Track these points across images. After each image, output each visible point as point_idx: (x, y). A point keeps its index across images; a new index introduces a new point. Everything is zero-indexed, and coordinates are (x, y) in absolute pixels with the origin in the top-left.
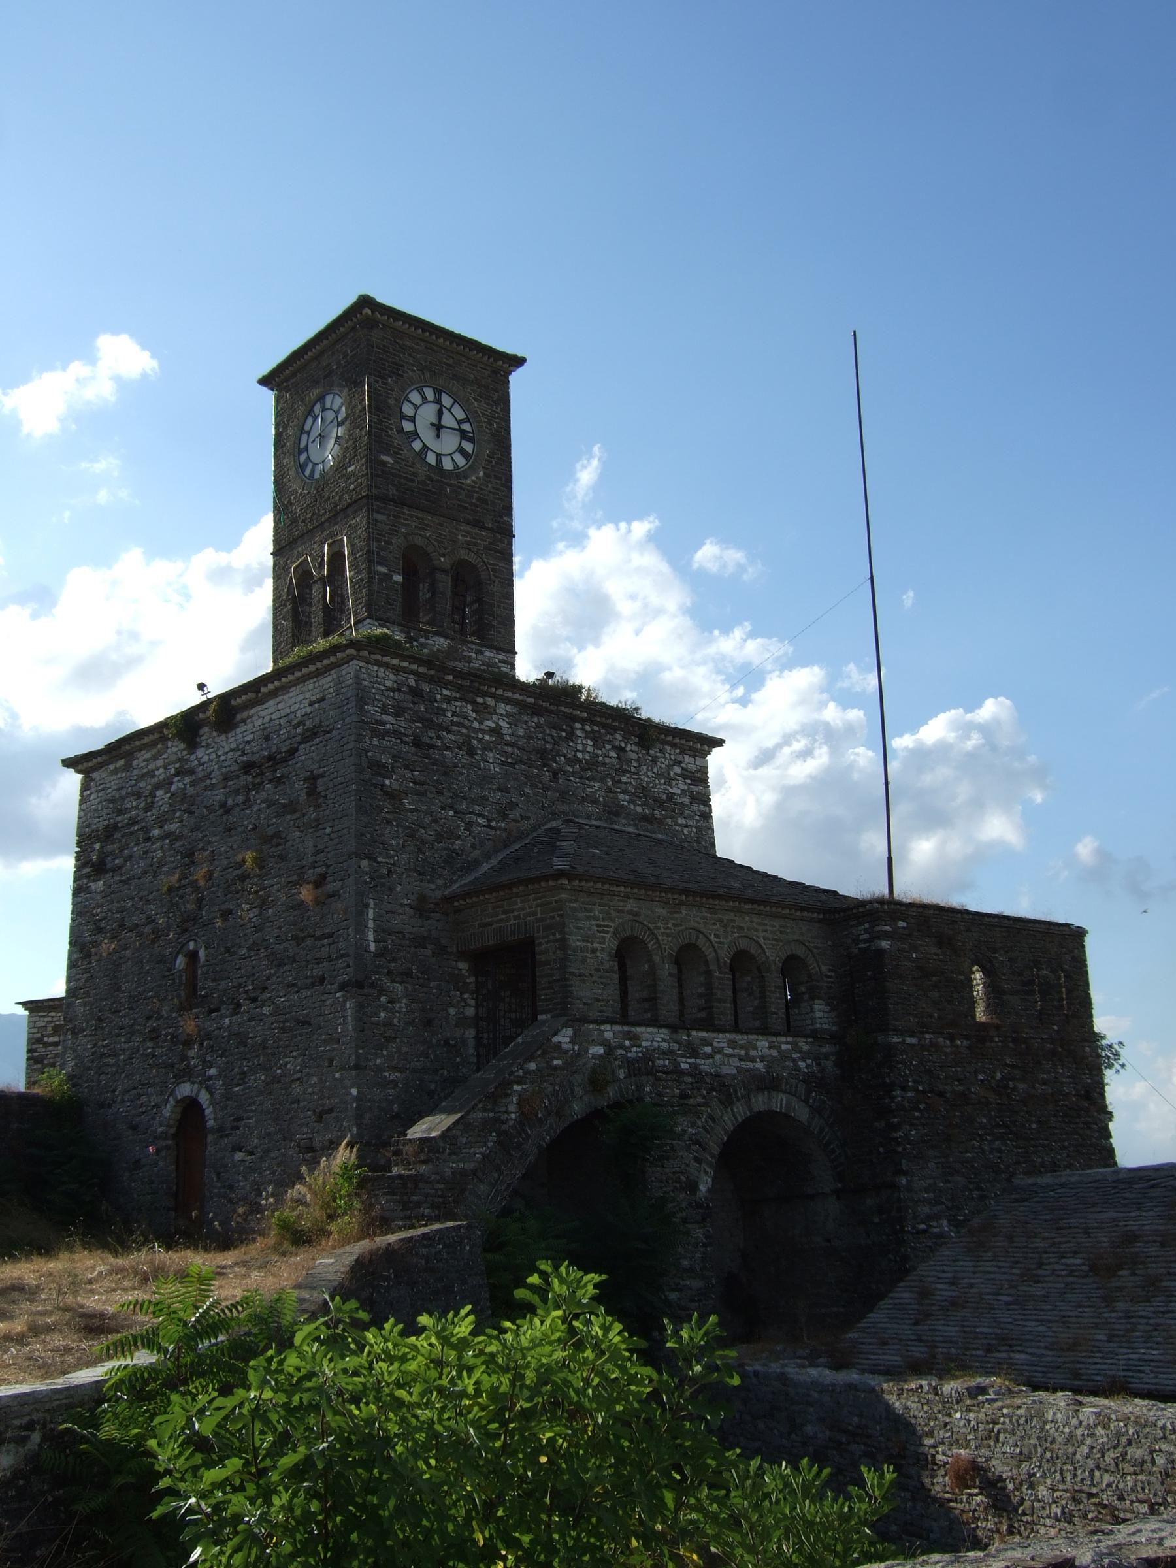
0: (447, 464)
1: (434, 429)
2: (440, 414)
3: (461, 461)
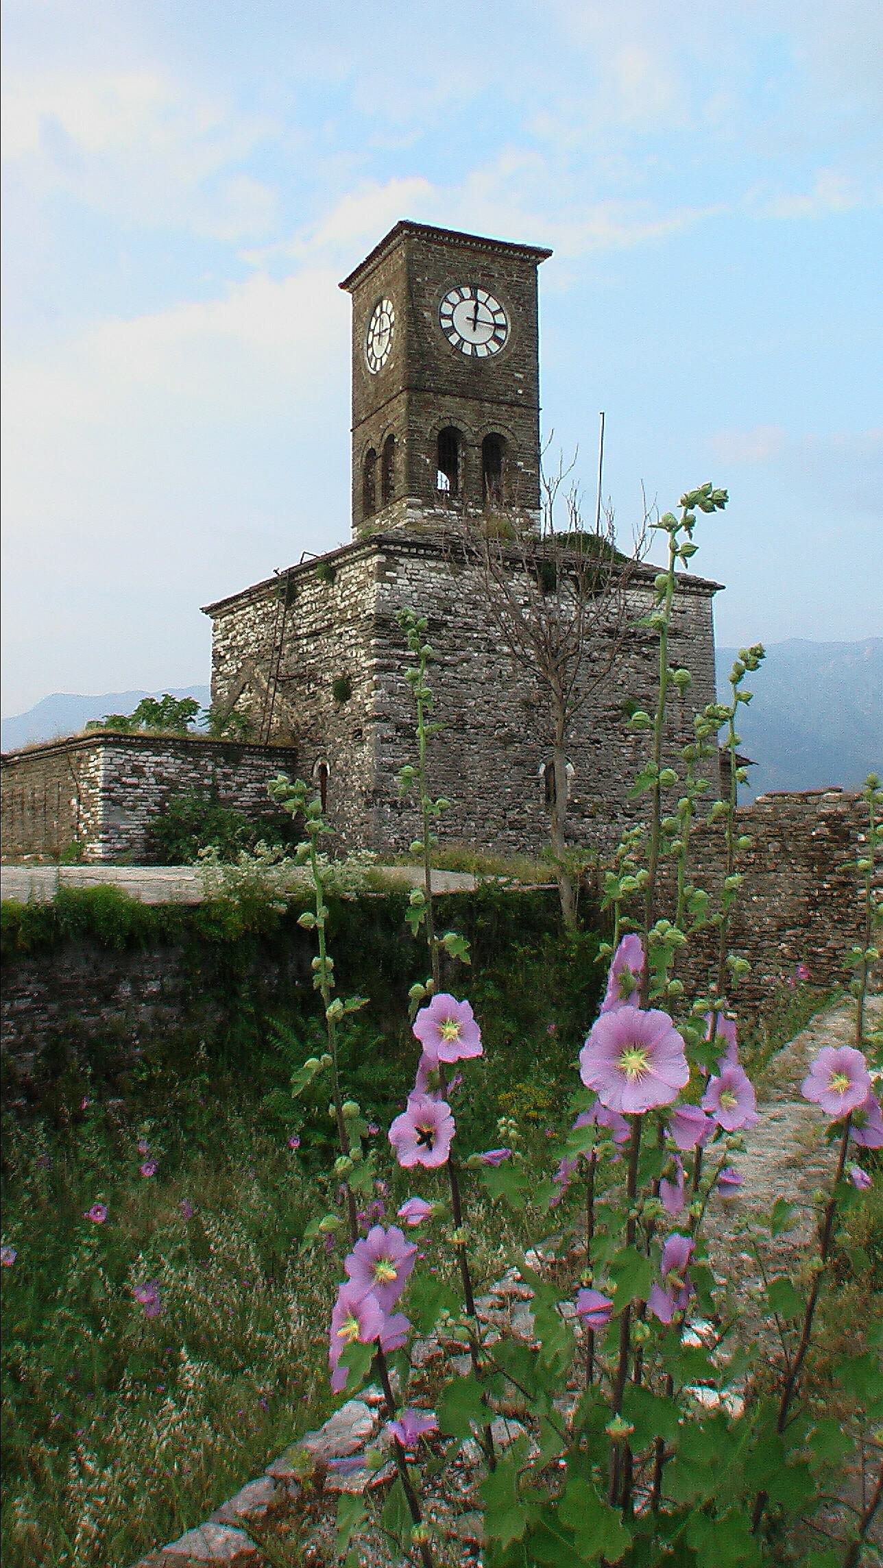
0: (482, 352)
1: (472, 322)
2: (476, 308)
3: (494, 347)
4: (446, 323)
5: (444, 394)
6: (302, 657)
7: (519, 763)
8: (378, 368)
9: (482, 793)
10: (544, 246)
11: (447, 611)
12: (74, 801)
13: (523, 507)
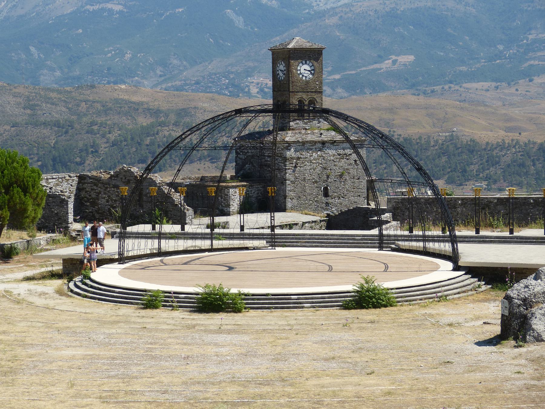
3: (311, 76)
4: (299, 72)
5: (298, 92)
6: (266, 161)
7: (317, 187)
9: (310, 194)
10: (324, 46)
11: (301, 155)
12: (220, 198)
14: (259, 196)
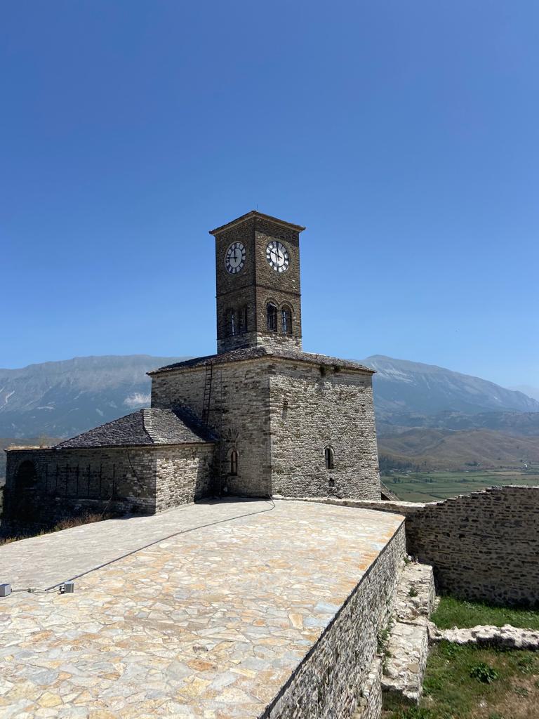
5: (268, 288)
8: (234, 272)
12: (129, 475)
13: (296, 337)
14: (206, 470)
